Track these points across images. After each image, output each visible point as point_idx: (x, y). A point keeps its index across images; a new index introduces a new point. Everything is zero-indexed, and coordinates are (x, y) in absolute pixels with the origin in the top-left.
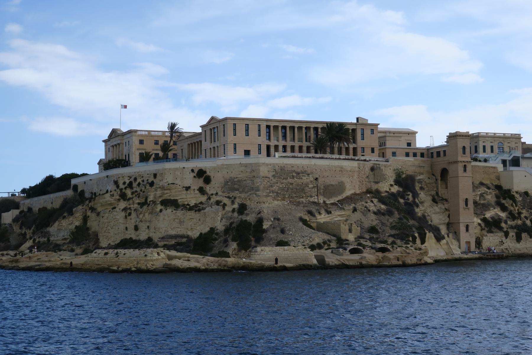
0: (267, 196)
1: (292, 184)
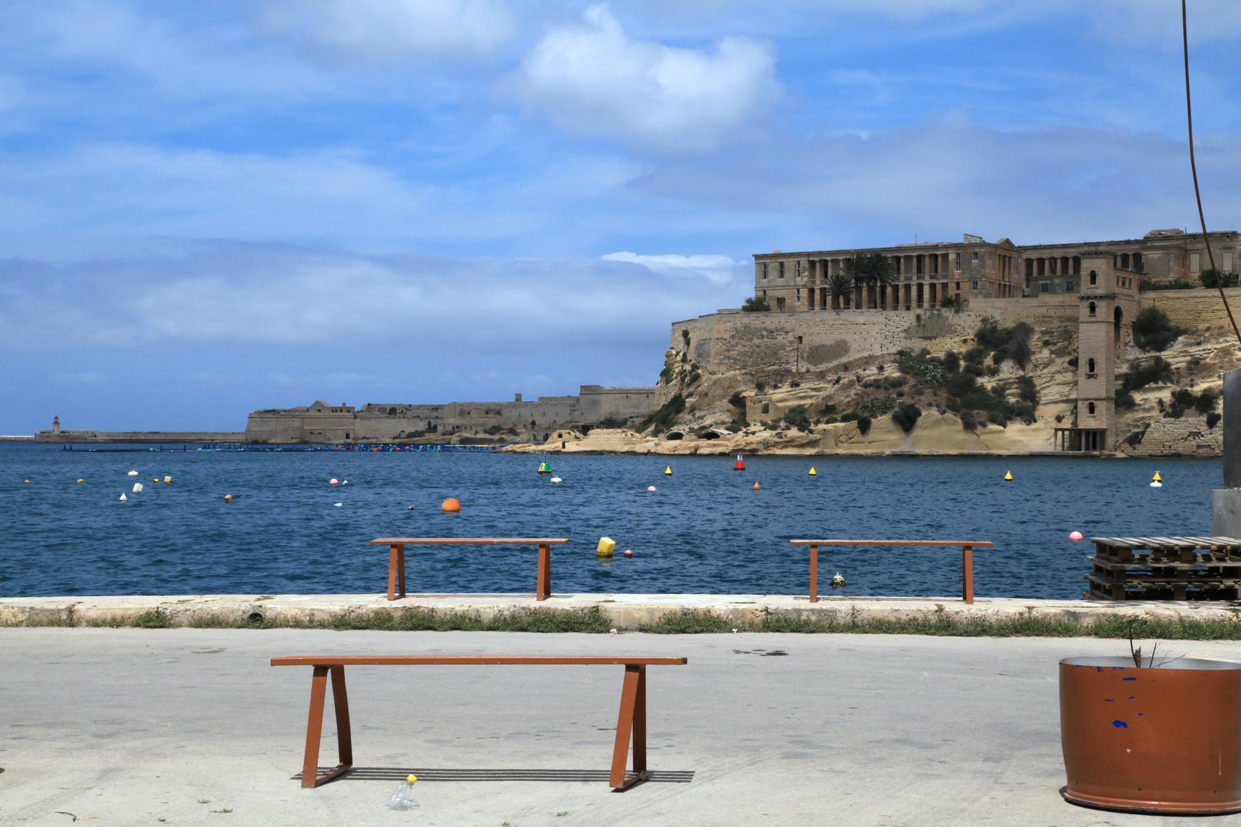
0: (720, 364)
1: (759, 346)
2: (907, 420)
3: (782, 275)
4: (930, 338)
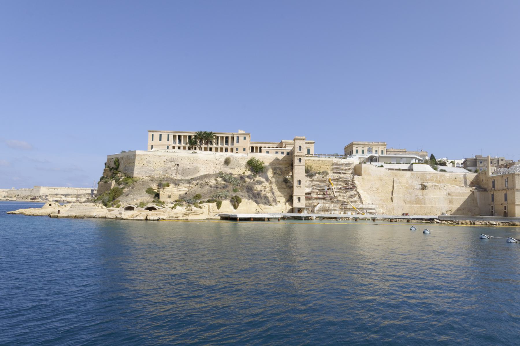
2: (236, 202)
3: (160, 140)
4: (232, 168)
